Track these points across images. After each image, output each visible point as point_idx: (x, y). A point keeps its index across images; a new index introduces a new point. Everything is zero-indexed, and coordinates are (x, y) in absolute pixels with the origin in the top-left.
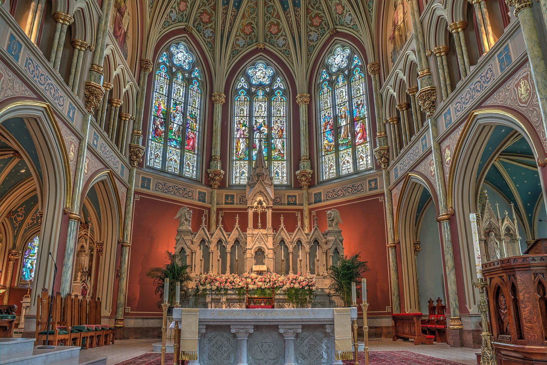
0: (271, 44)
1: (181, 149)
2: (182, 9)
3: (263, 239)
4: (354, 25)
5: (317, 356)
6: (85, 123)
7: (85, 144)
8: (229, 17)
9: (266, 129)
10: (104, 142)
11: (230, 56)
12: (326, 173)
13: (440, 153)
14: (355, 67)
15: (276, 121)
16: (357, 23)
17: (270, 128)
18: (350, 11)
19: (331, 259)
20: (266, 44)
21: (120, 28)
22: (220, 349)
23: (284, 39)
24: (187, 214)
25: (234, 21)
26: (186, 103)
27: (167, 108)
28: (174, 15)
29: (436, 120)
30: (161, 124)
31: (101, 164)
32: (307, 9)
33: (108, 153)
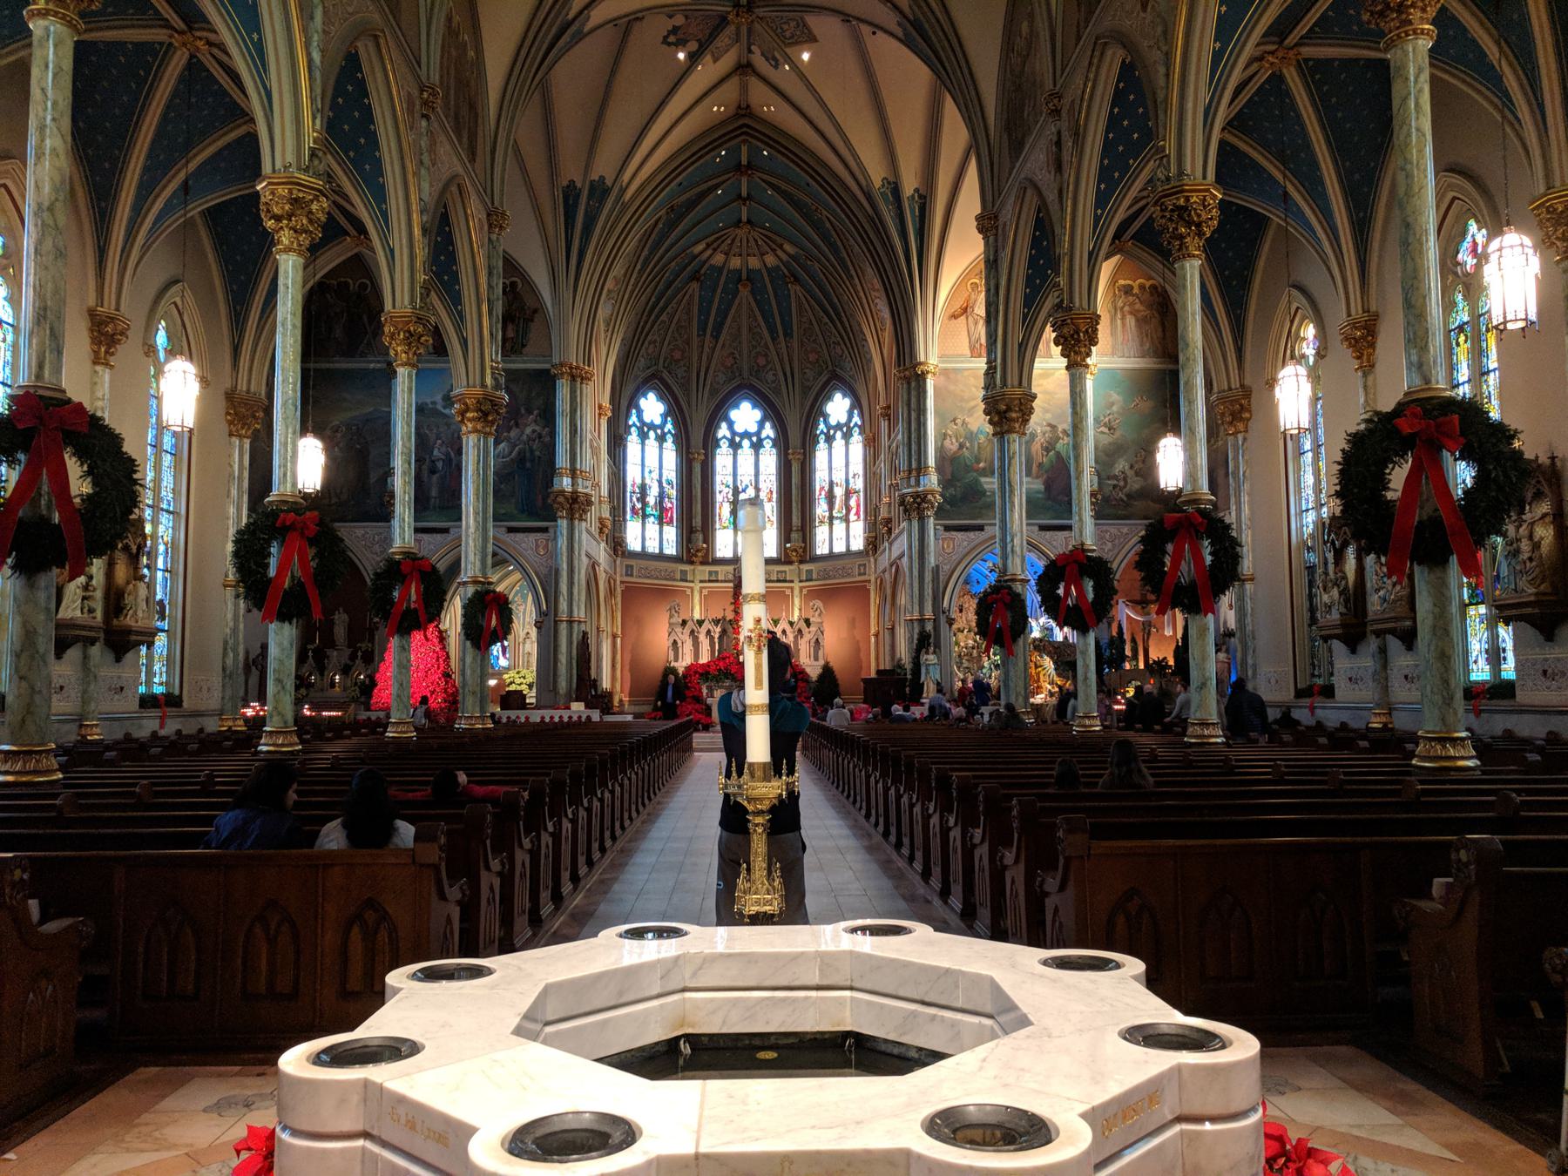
17: (757, 489)
29: (891, 544)
30: (638, 499)
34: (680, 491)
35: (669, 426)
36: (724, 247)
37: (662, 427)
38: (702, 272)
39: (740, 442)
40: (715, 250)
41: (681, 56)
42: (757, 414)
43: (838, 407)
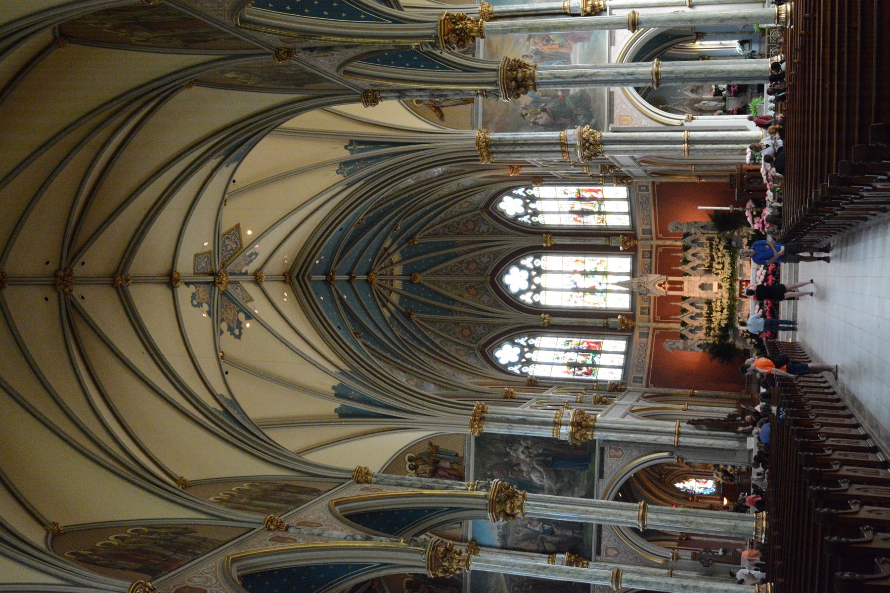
0: (486, 269)
1: (600, 354)
8: (463, 309)
17: (575, 272)
23: (483, 257)
25: (466, 304)
26: (555, 350)
30: (580, 370)
32: (458, 234)
35: (522, 341)
36: (386, 293)
37: (522, 347)
38: (404, 310)
39: (536, 285)
40: (388, 300)
41: (248, 325)
42: (514, 270)
43: (510, 206)
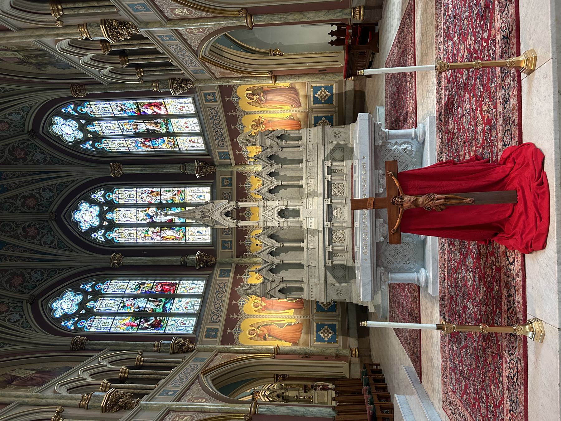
0: (50, 205)
2: (6, 309)
3: (269, 210)
4: (23, 111)
5: (404, 154)
6: (150, 407)
7: (174, 405)
9: (151, 209)
10: (170, 383)
11: (65, 250)
12: (198, 147)
13: (178, 21)
14: (77, 112)
15: (142, 198)
16: (21, 106)
17: (150, 205)
18: (5, 115)
19: (288, 143)
20: (49, 211)
21: (32, 379)
22: (399, 252)
23: (43, 191)
24: (244, 288)
25: (21, 247)
26: (123, 296)
27: (129, 316)
28: (14, 317)
30: (147, 321)
31: (194, 384)
33: (182, 377)
34: (147, 277)
35: (88, 287)
37: (85, 293)
39: (108, 221)
42: (85, 206)
